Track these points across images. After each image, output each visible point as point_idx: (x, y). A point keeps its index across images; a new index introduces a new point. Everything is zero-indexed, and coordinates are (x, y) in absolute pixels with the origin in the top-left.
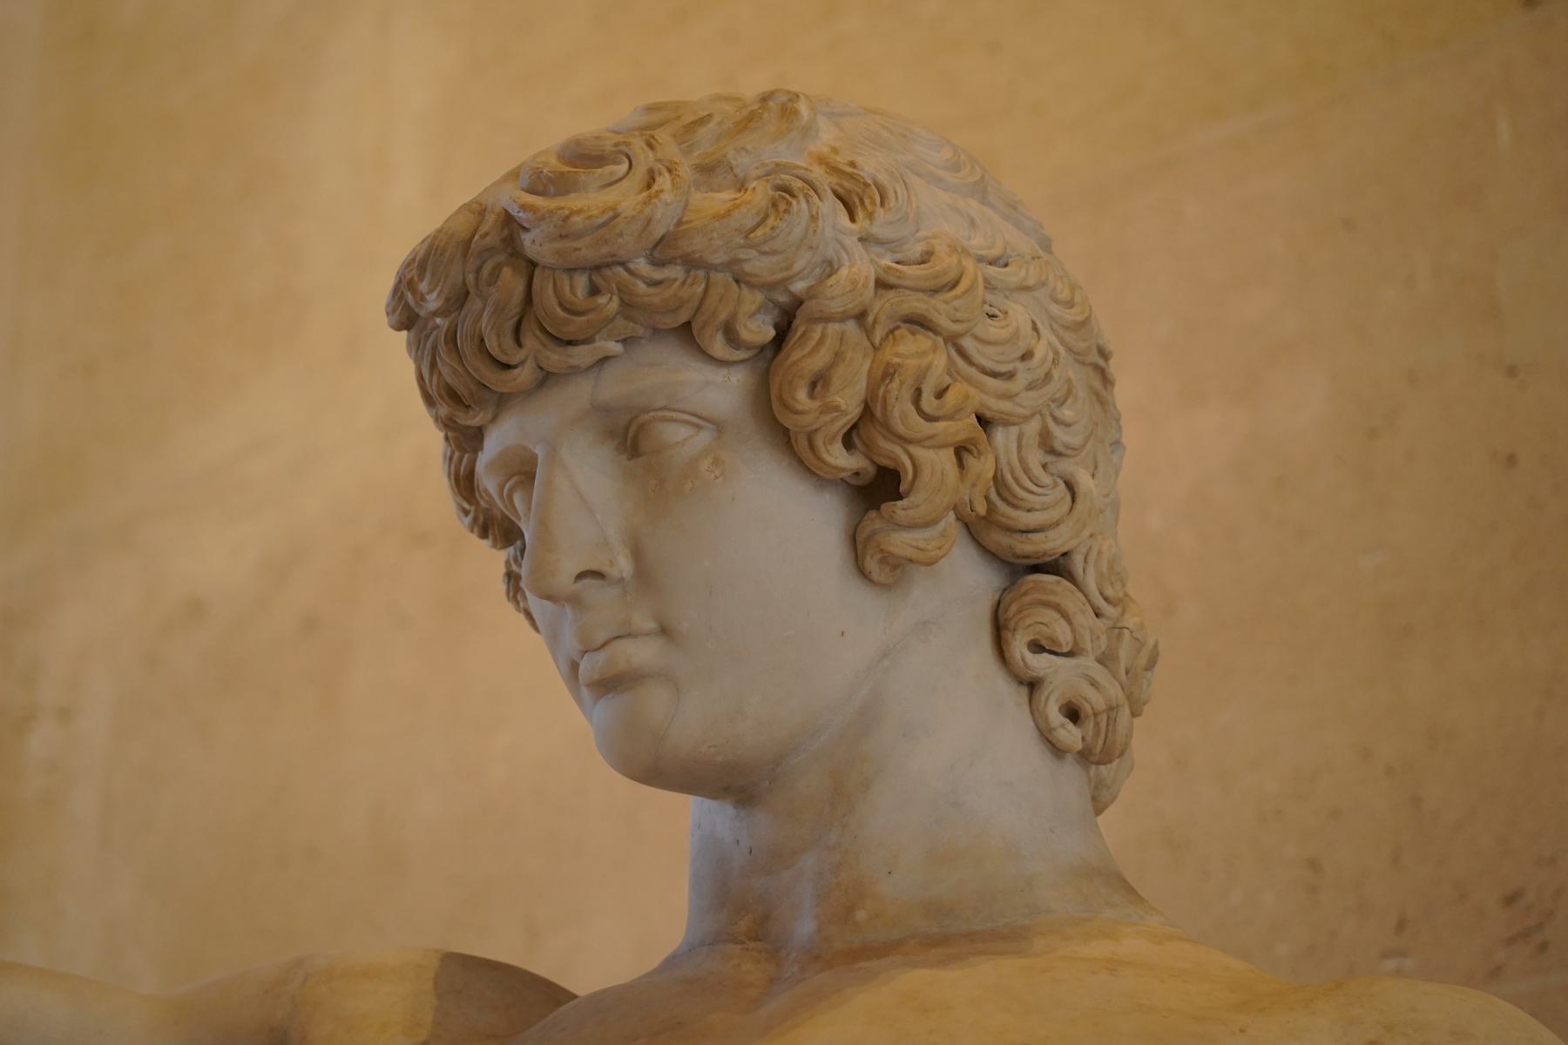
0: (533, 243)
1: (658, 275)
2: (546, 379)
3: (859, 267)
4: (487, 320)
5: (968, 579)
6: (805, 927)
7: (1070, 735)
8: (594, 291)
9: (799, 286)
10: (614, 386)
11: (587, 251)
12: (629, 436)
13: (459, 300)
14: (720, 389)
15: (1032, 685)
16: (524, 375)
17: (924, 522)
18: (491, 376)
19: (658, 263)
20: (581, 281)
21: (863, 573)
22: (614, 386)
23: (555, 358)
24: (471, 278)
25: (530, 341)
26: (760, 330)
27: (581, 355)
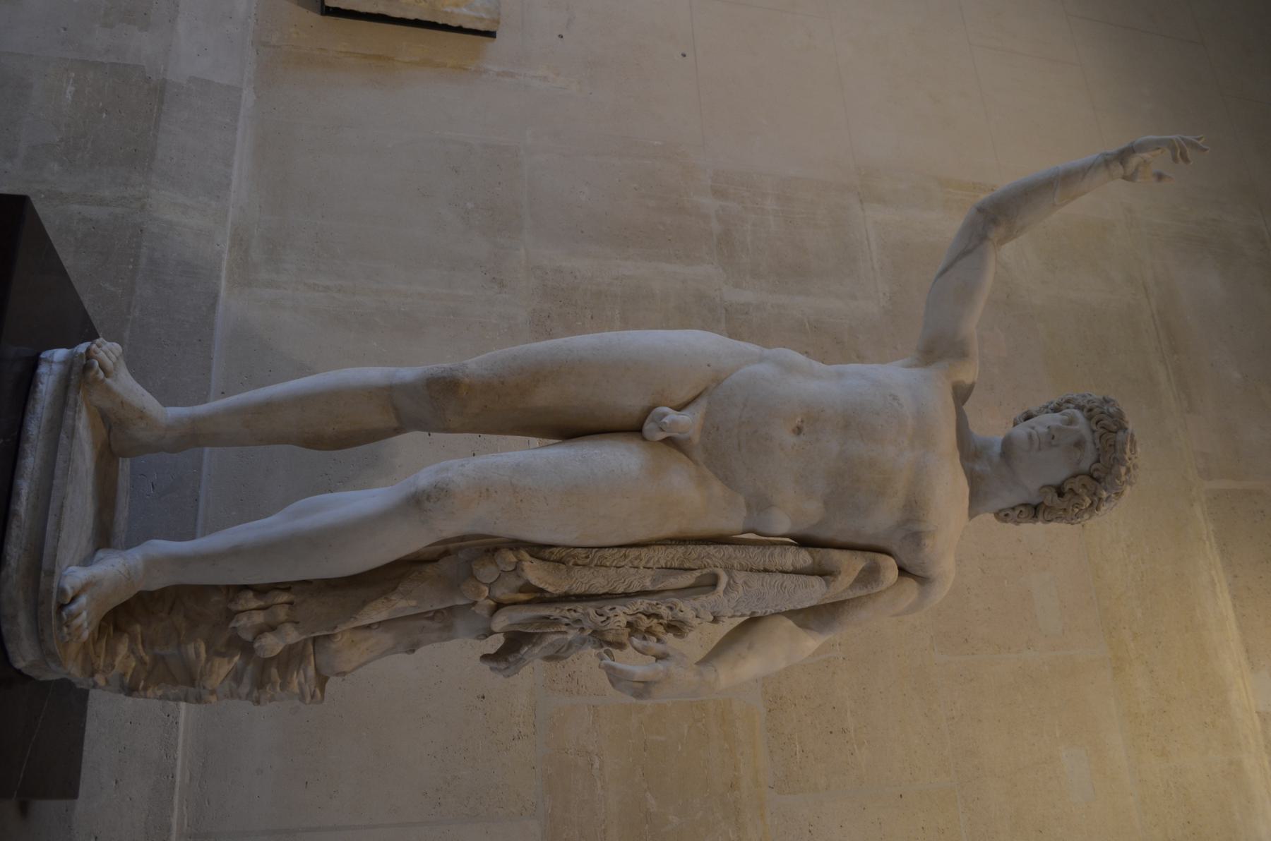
0: (1121, 433)
2: (1093, 432)
3: (1105, 494)
4: (1107, 421)
5: (1036, 501)
6: (977, 468)
7: (1002, 514)
11: (1118, 447)
12: (1079, 444)
13: (1111, 416)
14: (1085, 466)
15: (1013, 509)
17: (1052, 498)
18: (1094, 420)
21: (1043, 487)
22: (1089, 446)
23: (1097, 435)
25: (1102, 431)
26: (1096, 475)
27: (1097, 441)
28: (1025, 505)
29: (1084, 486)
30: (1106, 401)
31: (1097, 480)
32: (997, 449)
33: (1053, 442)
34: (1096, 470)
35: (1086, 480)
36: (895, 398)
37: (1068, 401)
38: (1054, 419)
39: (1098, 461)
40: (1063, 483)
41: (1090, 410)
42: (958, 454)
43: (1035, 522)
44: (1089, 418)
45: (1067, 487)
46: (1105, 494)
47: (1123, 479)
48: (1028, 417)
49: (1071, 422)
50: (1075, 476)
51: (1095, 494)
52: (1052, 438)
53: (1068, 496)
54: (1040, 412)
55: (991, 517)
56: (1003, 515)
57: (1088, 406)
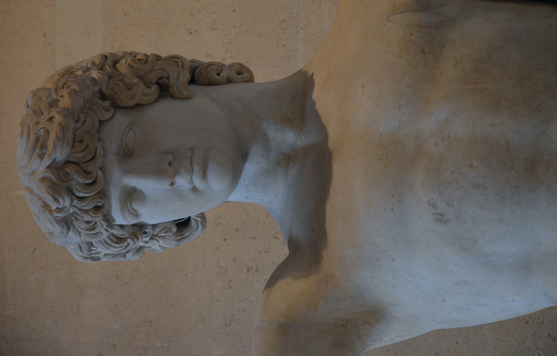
1: (82, 120)
7: (246, 75)
8: (81, 141)
9: (96, 89)
10: (112, 147)
11: (71, 135)
13: (71, 193)
14: (121, 121)
15: (229, 81)
16: (100, 172)
19: (77, 121)
20: (77, 144)
21: (187, 98)
22: (112, 147)
23: (99, 162)
24: (65, 185)
25: (91, 167)
27: (100, 151)
28: (212, 83)
29: (129, 87)
30: (67, 223)
31: (103, 97)
32: (250, 168)
33: (170, 158)
34: (107, 110)
35: (126, 100)
36: (440, 218)
37: (120, 240)
38: (149, 215)
39: (101, 122)
40: (156, 101)
41: (97, 208)
42: (331, 144)
43: (192, 61)
44: (103, 194)
45: (154, 89)
46: (95, 74)
47: (65, 92)
48: (183, 225)
49: (131, 195)
50: (138, 106)
51: (110, 77)
52: (169, 164)
53: (153, 77)
54: (165, 227)
55: (258, 79)
56: (242, 74)
57: (98, 219)
